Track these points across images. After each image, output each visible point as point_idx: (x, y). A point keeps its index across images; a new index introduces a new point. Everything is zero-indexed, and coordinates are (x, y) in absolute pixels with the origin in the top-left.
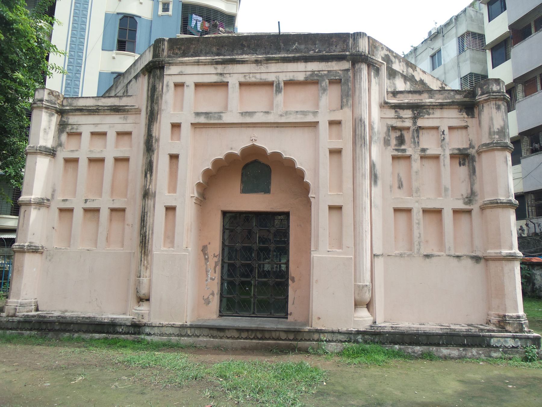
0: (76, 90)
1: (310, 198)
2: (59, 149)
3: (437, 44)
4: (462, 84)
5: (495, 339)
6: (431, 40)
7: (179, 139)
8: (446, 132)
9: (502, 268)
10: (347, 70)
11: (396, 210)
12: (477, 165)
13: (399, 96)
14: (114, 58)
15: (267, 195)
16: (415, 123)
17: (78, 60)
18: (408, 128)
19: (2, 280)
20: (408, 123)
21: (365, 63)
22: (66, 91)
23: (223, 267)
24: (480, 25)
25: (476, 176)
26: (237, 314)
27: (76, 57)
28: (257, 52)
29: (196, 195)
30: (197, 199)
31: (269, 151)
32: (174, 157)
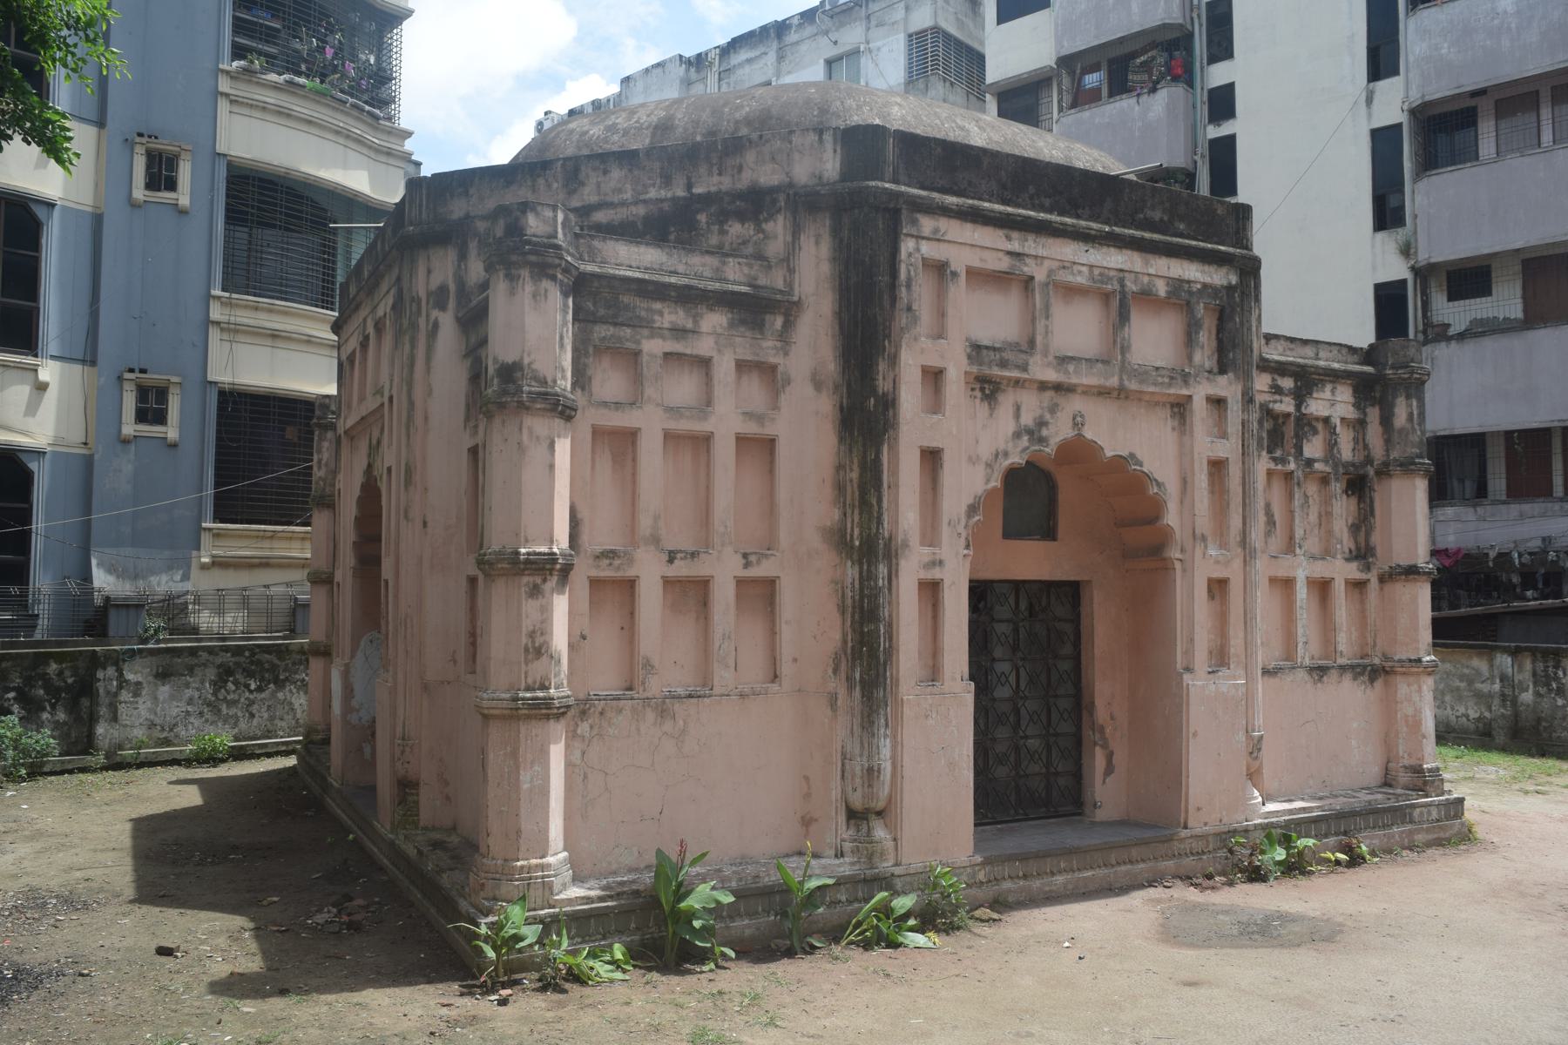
1: (1176, 562)
3: (852, 36)
5: (1418, 810)
6: (832, 17)
8: (1338, 430)
9: (1420, 687)
12: (1377, 497)
13: (1273, 342)
16: (1298, 407)
18: (1288, 415)
20: (1286, 406)
24: (960, 16)
25: (1374, 517)
26: (987, 817)
28: (1079, 212)
32: (932, 458)
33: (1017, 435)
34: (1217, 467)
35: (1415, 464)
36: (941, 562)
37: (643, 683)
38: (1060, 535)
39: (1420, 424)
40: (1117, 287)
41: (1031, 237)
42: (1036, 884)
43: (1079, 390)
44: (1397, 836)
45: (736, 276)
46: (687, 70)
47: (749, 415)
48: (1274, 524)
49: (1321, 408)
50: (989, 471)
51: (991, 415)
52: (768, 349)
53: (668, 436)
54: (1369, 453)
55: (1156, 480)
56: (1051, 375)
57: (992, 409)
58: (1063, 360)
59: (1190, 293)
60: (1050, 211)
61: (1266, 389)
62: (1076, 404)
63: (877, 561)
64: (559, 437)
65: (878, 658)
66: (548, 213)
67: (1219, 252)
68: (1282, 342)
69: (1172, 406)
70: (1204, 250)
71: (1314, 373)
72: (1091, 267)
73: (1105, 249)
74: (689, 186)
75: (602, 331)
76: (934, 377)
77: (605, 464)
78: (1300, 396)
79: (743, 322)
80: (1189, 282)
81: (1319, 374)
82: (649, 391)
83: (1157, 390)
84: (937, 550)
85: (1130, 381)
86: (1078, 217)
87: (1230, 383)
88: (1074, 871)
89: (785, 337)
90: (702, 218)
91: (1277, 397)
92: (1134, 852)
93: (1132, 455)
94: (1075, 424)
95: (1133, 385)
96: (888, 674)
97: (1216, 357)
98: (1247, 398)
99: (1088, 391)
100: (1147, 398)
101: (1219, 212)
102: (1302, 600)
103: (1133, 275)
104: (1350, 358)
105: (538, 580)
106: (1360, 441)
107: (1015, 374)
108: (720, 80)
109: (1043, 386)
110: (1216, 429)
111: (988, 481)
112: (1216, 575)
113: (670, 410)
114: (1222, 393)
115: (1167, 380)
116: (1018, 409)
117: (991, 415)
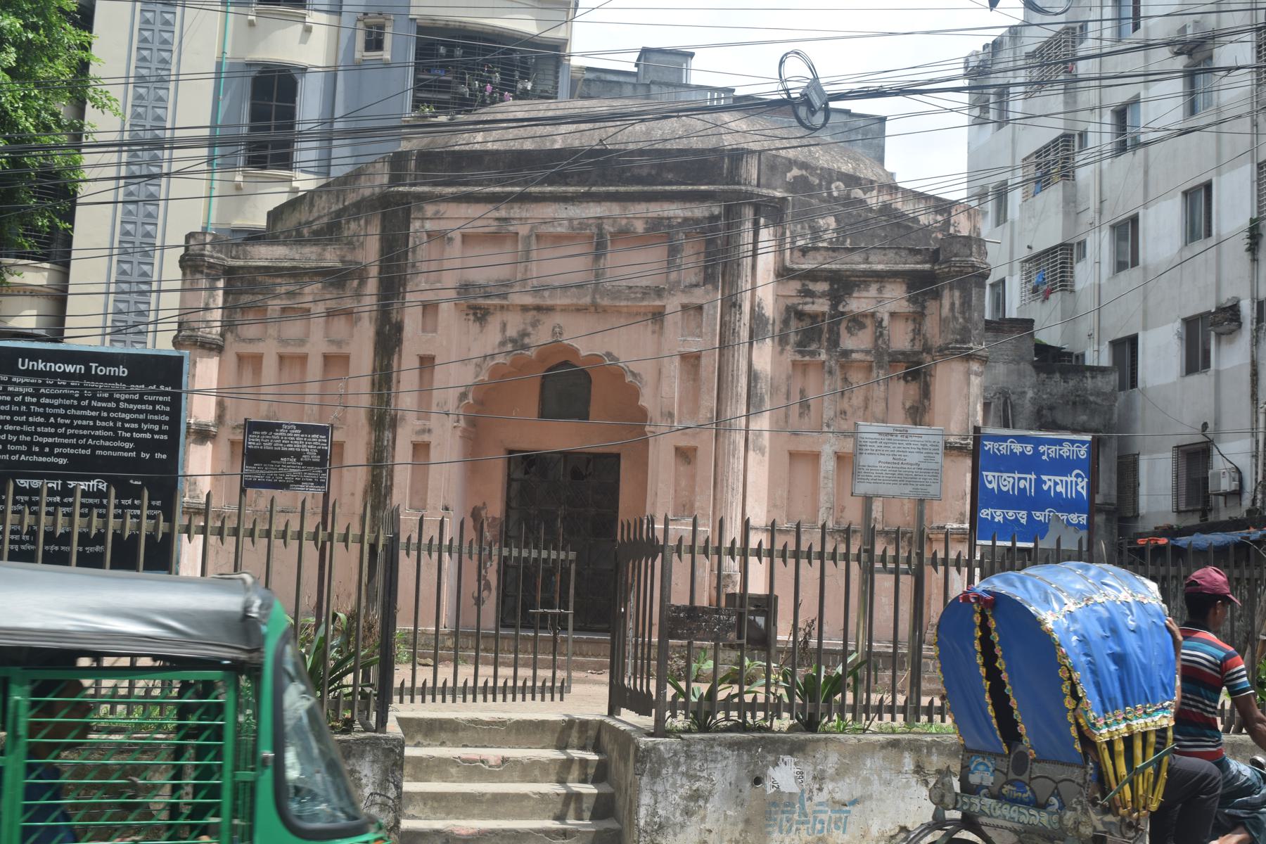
0: (159, 111)
2: (229, 336)
7: (435, 331)
8: (885, 323)
11: (793, 455)
13: (811, 254)
14: (251, 24)
15: (582, 424)
16: (834, 306)
17: (163, 33)
18: (824, 314)
20: (822, 306)
21: (750, 204)
25: (929, 400)
27: (158, 26)
29: (462, 423)
30: (465, 430)
31: (583, 353)
32: (427, 362)
33: (503, 344)
34: (691, 361)
35: (948, 349)
37: (255, 502)
39: (963, 313)
40: (594, 230)
41: (516, 206)
43: (558, 308)
44: (886, 679)
45: (331, 257)
48: (809, 407)
49: (864, 306)
50: (478, 369)
51: (481, 331)
53: (282, 358)
54: (926, 341)
55: (631, 372)
56: (528, 300)
57: (482, 327)
58: (537, 291)
59: (670, 227)
61: (794, 294)
62: (558, 319)
63: (384, 429)
64: (201, 357)
65: (380, 493)
66: (201, 237)
68: (822, 252)
70: (672, 192)
71: (850, 276)
72: (571, 220)
73: (585, 205)
74: (344, 201)
75: (246, 299)
78: (836, 298)
79: (332, 284)
80: (669, 218)
81: (857, 276)
83: (629, 303)
84: (427, 423)
85: (602, 298)
86: (567, 184)
87: (707, 292)
92: (585, 648)
93: (609, 354)
94: (554, 334)
95: (606, 302)
96: (388, 502)
97: (702, 274)
98: (730, 303)
99: (565, 309)
100: (625, 310)
102: (827, 472)
103: (611, 221)
104: (911, 259)
106: (917, 332)
107: (496, 301)
109: (525, 309)
110: (698, 331)
111: (477, 376)
112: (684, 442)
113: (283, 342)
115: (639, 295)
116: (504, 327)
117: (481, 331)
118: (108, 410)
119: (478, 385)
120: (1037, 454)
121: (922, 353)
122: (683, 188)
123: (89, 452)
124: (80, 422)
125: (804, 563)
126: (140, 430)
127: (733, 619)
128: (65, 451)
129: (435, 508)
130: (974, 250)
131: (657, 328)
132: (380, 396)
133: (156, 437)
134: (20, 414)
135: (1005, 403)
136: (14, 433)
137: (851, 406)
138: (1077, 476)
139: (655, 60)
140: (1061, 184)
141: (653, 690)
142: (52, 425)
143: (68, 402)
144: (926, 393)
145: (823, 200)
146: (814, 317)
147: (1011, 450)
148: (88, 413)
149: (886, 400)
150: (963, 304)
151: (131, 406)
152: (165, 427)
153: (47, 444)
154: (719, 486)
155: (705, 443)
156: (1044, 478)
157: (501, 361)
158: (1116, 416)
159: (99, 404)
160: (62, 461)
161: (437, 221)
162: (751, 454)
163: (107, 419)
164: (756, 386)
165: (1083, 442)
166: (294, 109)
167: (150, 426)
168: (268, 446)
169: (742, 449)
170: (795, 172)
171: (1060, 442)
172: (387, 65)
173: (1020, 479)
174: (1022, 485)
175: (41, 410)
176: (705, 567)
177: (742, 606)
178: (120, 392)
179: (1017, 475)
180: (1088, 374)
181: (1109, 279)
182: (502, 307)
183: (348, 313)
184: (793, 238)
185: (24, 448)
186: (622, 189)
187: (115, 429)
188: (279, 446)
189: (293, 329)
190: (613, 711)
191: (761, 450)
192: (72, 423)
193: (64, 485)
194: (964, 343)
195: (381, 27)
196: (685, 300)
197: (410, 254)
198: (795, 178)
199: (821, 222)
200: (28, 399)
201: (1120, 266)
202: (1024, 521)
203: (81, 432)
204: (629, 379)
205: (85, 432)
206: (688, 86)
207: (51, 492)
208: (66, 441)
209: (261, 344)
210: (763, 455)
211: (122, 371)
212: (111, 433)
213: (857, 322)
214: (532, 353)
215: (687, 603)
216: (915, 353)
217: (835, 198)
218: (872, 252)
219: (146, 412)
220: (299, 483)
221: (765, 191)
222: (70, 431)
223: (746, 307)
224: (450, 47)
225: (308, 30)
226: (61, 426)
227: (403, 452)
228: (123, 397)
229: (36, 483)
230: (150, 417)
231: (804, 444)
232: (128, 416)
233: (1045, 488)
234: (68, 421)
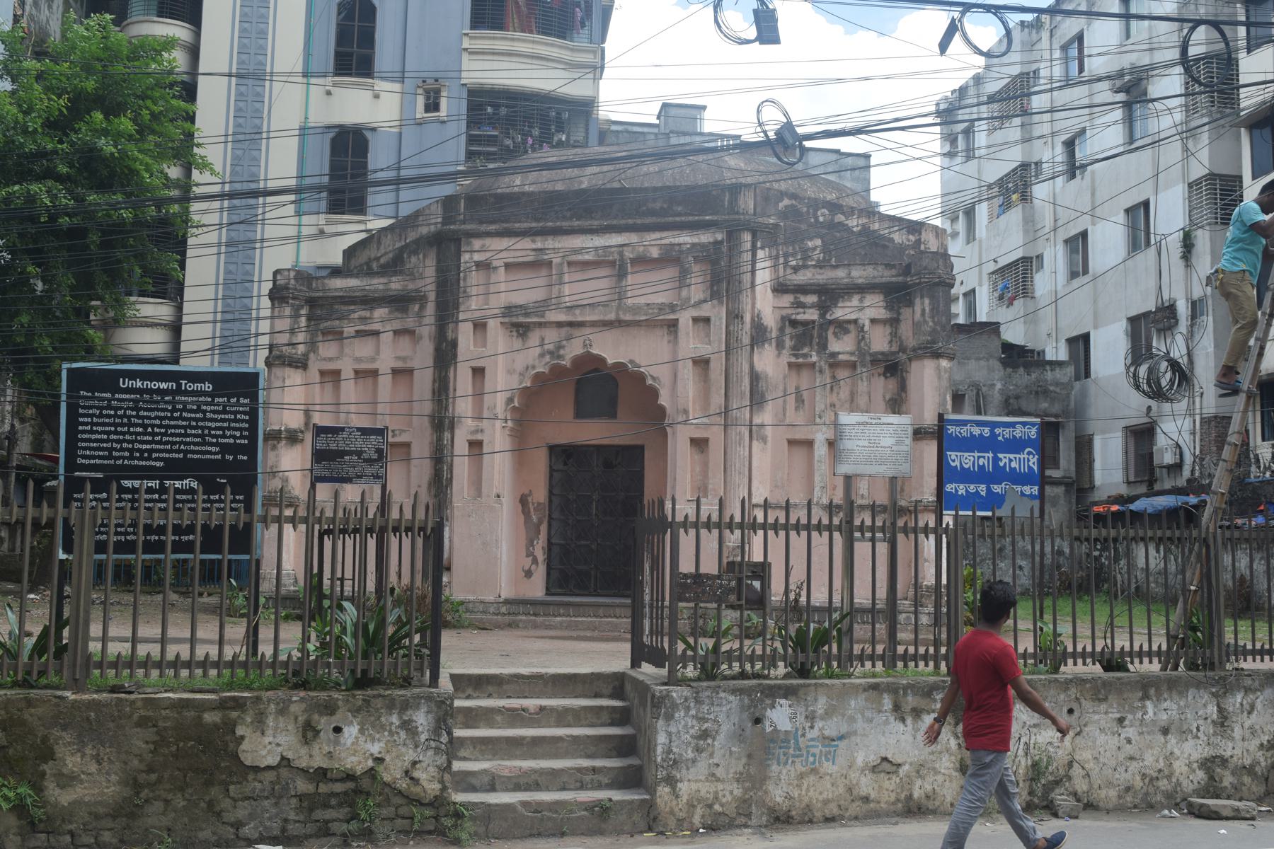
2: (312, 355)
4: (1188, 83)
5: (904, 615)
8: (866, 328)
10: (721, 242)
11: (791, 442)
16: (822, 315)
17: (255, 104)
18: (813, 322)
19: (219, 551)
20: (812, 315)
21: (748, 230)
22: (233, 173)
23: (550, 526)
30: (512, 429)
31: (610, 361)
32: (478, 372)
33: (542, 355)
34: (702, 363)
36: (482, 431)
38: (619, 415)
39: (932, 317)
40: (617, 257)
42: (540, 619)
45: (396, 285)
46: (1030, 34)
47: (398, 358)
48: (803, 401)
52: (410, 322)
53: (357, 372)
56: (562, 317)
58: (570, 308)
59: (681, 252)
60: (571, 219)
66: (286, 273)
67: (704, 221)
68: (811, 269)
69: (669, 326)
70: (682, 222)
72: (596, 249)
73: (608, 235)
76: (479, 326)
77: (329, 387)
78: (823, 308)
79: (397, 310)
80: (680, 245)
82: (347, 350)
85: (624, 314)
86: (592, 218)
87: (714, 307)
88: (569, 615)
89: (420, 315)
90: (405, 256)
91: (801, 310)
92: (618, 611)
93: (631, 362)
94: (585, 346)
95: (628, 317)
97: (709, 292)
101: (714, 193)
103: (630, 248)
104: (887, 273)
105: (275, 442)
106: (894, 335)
108: (1051, 36)
109: (560, 325)
111: (521, 383)
114: (707, 314)
115: (656, 311)
118: (197, 420)
119: (524, 391)
120: (994, 436)
121: (898, 353)
122: (691, 218)
123: (181, 456)
124: (173, 431)
125: (793, 534)
126: (224, 436)
127: (733, 583)
128: (161, 455)
129: (489, 496)
130: (940, 263)
131: (672, 338)
132: (440, 401)
133: (238, 441)
134: (122, 425)
135: (978, 394)
136: (118, 441)
137: (839, 400)
138: (1029, 453)
139: (673, 112)
140: (1020, 206)
141: (666, 646)
142: (150, 434)
143: (162, 414)
144: (903, 387)
145: (811, 225)
146: (805, 323)
147: (971, 433)
148: (180, 423)
149: (869, 394)
150: (932, 310)
151: (216, 416)
152: (245, 433)
153: (146, 450)
154: (728, 470)
155: (716, 436)
156: (1000, 456)
157: (541, 370)
158: (1072, 404)
159: (189, 415)
160: (159, 464)
161: (483, 254)
162: (755, 443)
163: (196, 428)
164: (757, 386)
165: (1033, 425)
166: (366, 163)
167: (233, 433)
168: (333, 447)
169: (747, 439)
170: (786, 202)
171: (1013, 425)
172: (443, 122)
173: (979, 457)
174: (981, 462)
175: (140, 421)
176: (710, 541)
177: (740, 572)
178: (207, 404)
179: (976, 454)
180: (1048, 368)
181: (1064, 286)
182: (540, 325)
183: (409, 332)
184: (786, 256)
185: (127, 454)
186: (639, 221)
187: (203, 436)
188: (342, 447)
189: (363, 349)
190: (635, 664)
191: (764, 439)
192: (166, 431)
193: (162, 484)
194: (934, 343)
195: (438, 92)
196: (696, 313)
197: (461, 282)
198: (786, 207)
199: (810, 244)
200: (129, 412)
201: (1073, 275)
202: (983, 494)
203: (174, 439)
204: (650, 382)
205: (178, 439)
206: (701, 134)
207: (150, 490)
208: (162, 447)
209: (339, 362)
210: (765, 443)
211: (208, 387)
212: (199, 440)
213: (842, 327)
214: (566, 362)
215: (693, 570)
216: (893, 353)
217: (821, 223)
218: (853, 268)
219: (229, 420)
220: (360, 477)
221: (760, 220)
222: (165, 439)
223: (748, 318)
224: (496, 106)
225: (377, 97)
226: (157, 434)
227: (461, 446)
228: (209, 408)
229: (137, 483)
230: (232, 425)
231: (799, 435)
232: (213, 425)
233: (1001, 464)
234: (163, 431)
